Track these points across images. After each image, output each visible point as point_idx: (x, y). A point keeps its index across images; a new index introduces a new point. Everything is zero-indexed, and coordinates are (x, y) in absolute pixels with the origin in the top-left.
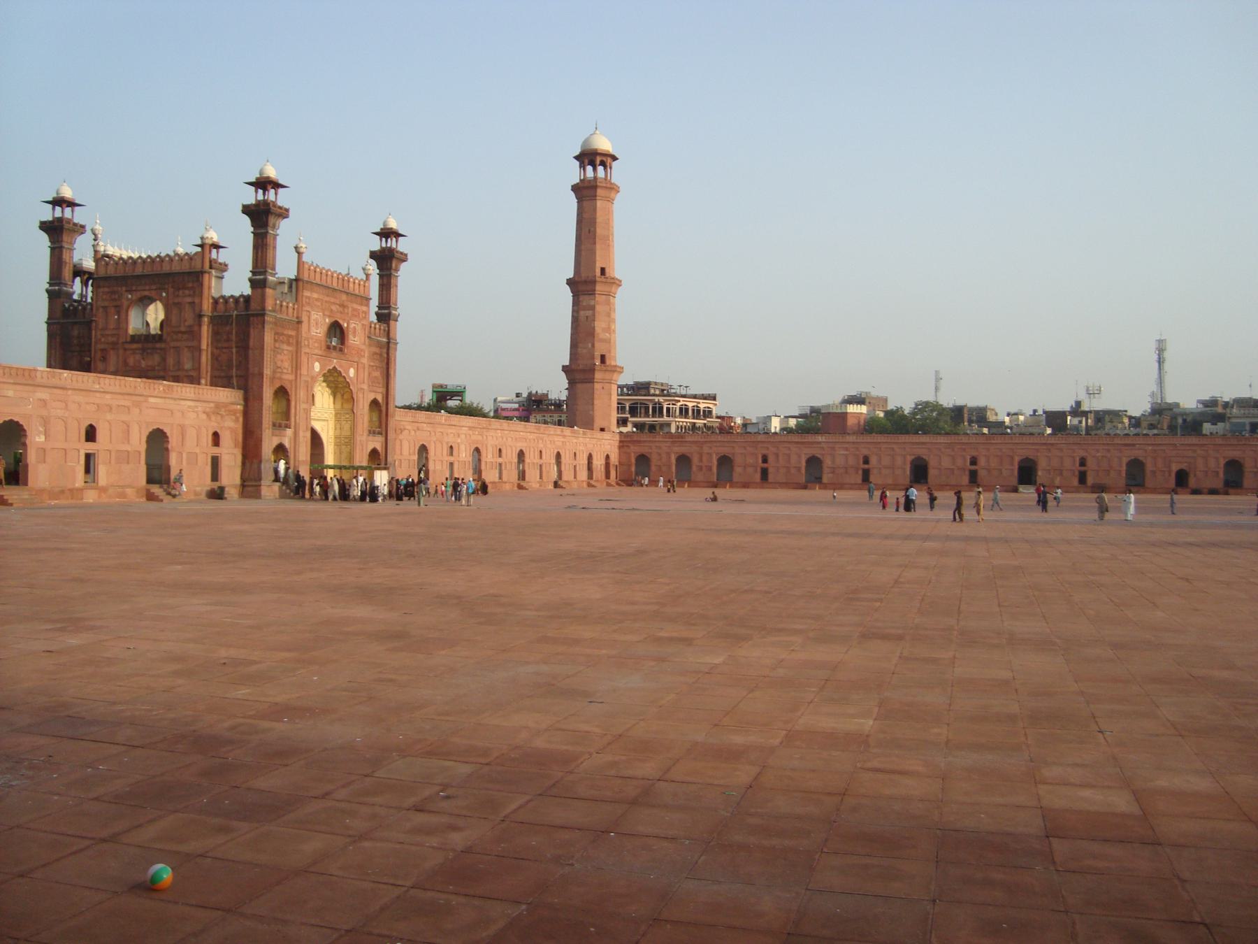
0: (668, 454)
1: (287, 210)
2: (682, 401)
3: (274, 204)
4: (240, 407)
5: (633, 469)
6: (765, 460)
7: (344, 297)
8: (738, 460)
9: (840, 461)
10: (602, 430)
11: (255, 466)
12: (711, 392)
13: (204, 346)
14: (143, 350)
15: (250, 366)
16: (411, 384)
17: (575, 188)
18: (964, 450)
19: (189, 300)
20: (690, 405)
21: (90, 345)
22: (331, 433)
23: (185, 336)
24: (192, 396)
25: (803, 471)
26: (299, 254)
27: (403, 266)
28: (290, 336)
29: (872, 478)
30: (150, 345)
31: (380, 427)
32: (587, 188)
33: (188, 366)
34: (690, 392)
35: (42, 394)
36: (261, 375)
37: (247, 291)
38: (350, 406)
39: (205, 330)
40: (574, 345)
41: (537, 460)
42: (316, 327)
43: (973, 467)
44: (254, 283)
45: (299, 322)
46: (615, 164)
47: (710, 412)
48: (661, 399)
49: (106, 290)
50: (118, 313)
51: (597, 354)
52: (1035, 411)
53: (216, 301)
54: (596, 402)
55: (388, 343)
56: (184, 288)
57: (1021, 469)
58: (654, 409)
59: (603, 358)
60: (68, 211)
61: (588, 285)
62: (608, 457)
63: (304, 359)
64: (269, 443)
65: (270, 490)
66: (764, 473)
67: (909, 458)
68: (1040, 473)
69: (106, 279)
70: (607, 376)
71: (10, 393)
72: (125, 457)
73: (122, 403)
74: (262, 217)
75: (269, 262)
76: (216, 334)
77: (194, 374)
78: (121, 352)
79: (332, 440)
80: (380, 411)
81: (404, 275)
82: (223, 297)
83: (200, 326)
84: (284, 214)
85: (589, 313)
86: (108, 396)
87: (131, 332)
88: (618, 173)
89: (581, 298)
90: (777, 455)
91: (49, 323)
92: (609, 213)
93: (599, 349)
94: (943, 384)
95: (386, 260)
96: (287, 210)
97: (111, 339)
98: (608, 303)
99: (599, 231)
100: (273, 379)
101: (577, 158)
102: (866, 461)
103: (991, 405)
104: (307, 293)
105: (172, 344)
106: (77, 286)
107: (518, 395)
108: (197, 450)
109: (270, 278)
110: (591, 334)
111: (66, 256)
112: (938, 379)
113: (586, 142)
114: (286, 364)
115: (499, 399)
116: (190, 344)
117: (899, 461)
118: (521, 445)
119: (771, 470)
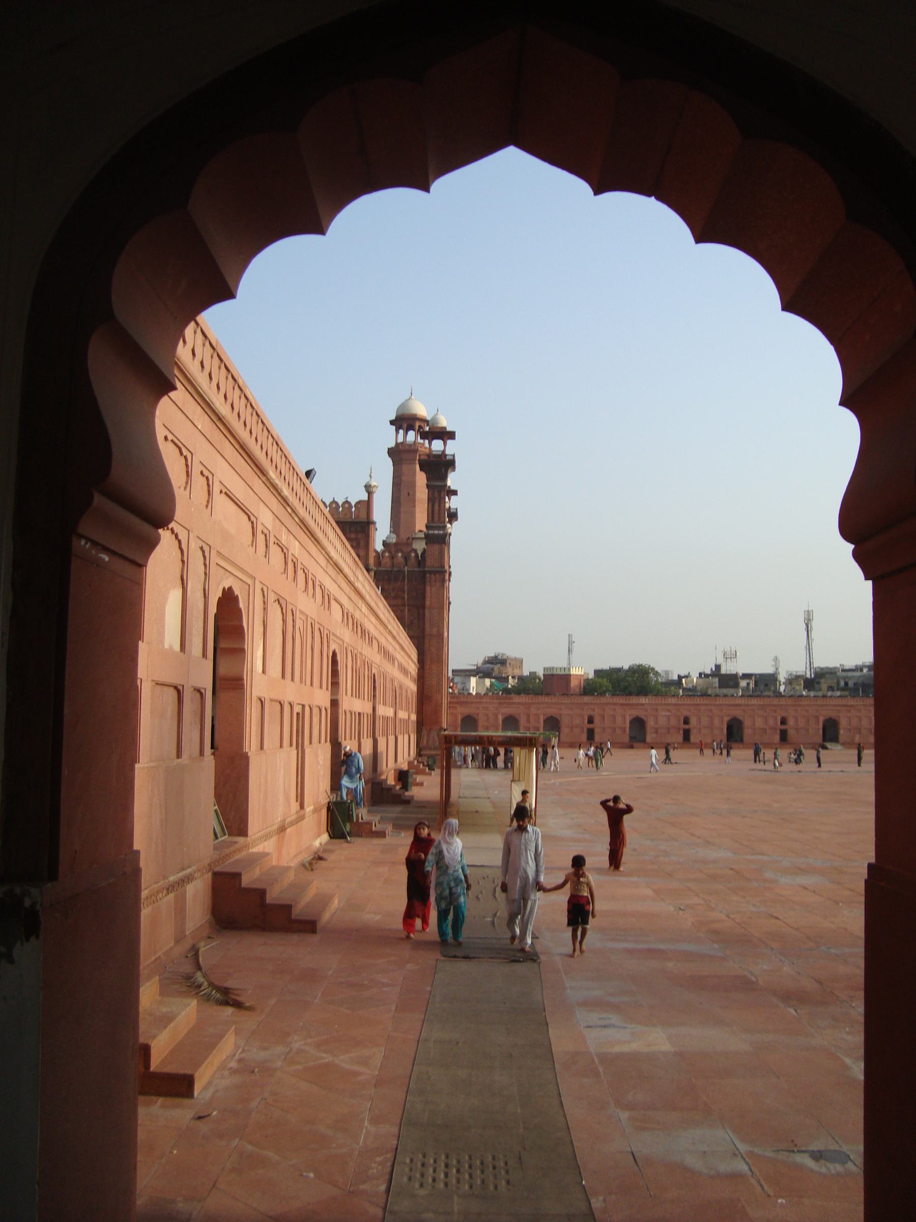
0: (496, 715)
6: (591, 720)
8: (565, 721)
9: (662, 721)
15: (427, 626)
17: (391, 452)
18: (775, 711)
25: (628, 729)
43: (784, 727)
52: (700, 674)
57: (730, 728)
66: (591, 734)
67: (726, 719)
68: (842, 732)
94: (575, 647)
101: (392, 423)
102: (686, 721)
112: (571, 643)
113: (403, 406)
119: (597, 731)
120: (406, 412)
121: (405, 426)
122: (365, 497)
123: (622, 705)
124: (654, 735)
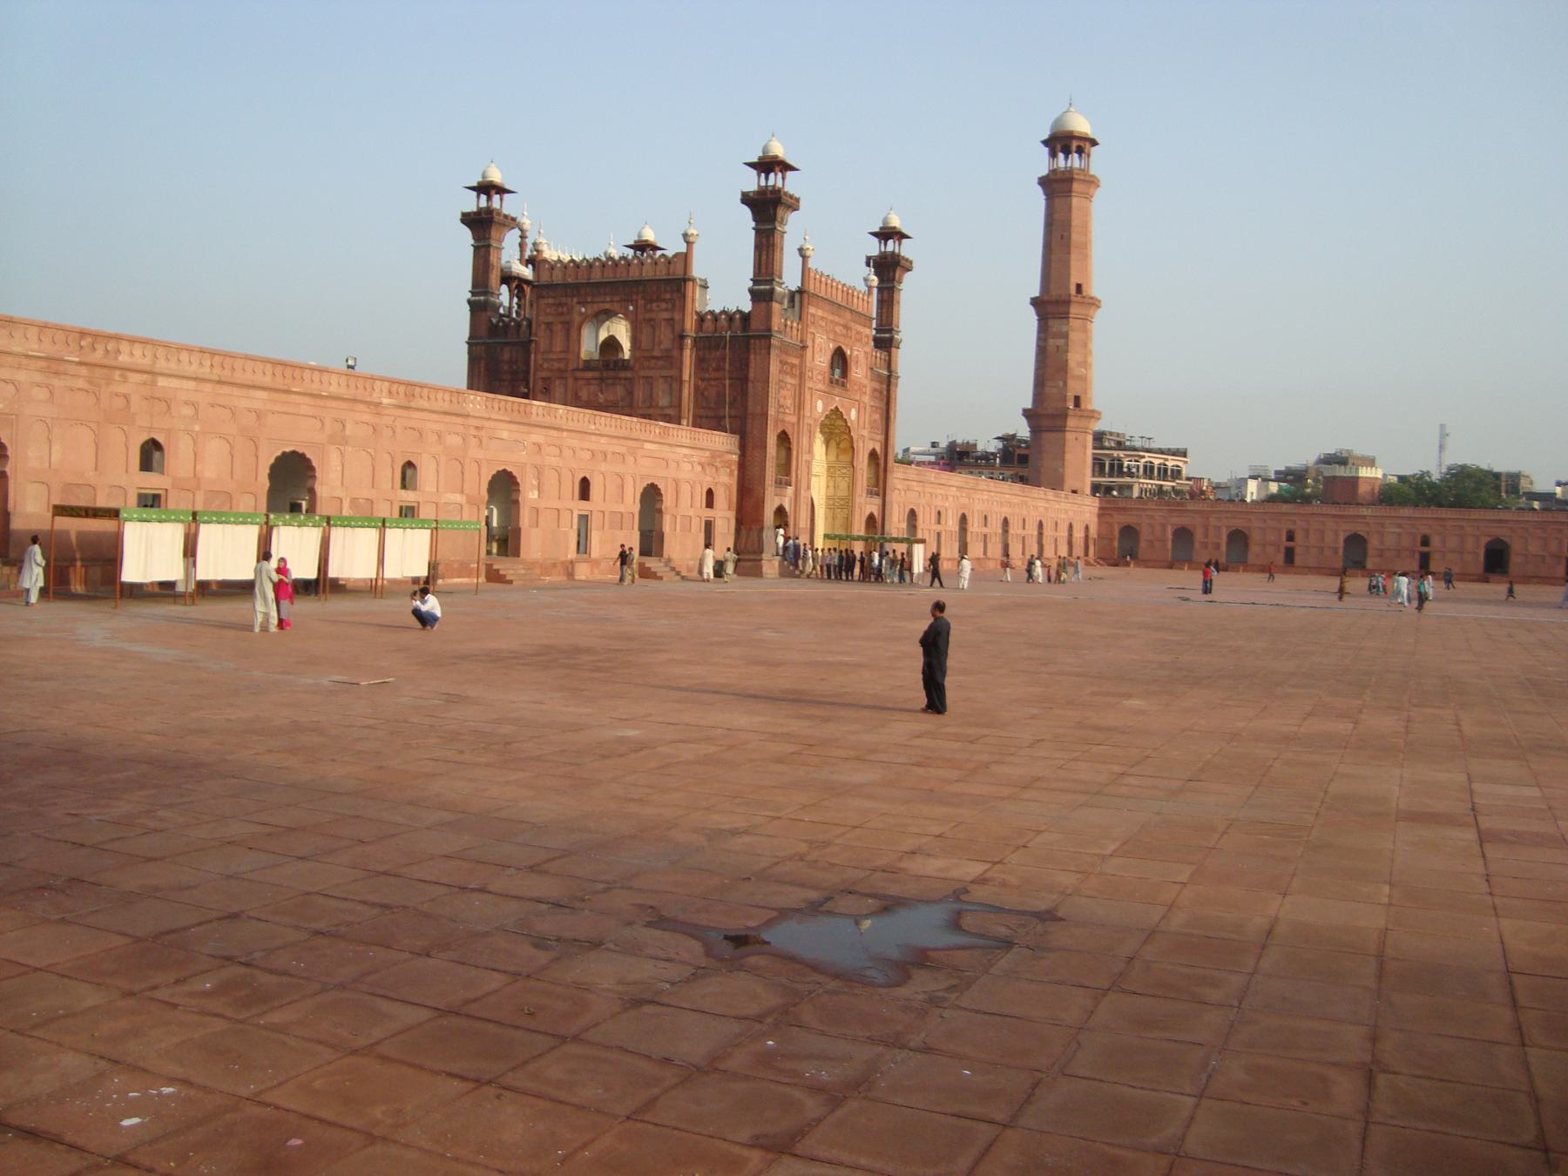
0: (1164, 527)
1: (798, 200)
2: (1148, 457)
4: (735, 458)
5: (1116, 544)
6: (1291, 537)
7: (848, 315)
8: (1255, 536)
10: (1074, 492)
11: (754, 534)
13: (686, 377)
14: (602, 379)
16: (916, 431)
17: (1044, 182)
18: (1560, 531)
19: (666, 315)
20: (1156, 462)
21: (528, 372)
22: (823, 492)
23: (661, 363)
24: (687, 442)
26: (804, 257)
27: (907, 276)
28: (793, 366)
30: (611, 373)
31: (877, 485)
32: (1057, 181)
33: (663, 401)
34: (1154, 445)
35: (537, 437)
36: (765, 415)
37: (746, 306)
38: (846, 458)
39: (688, 356)
40: (1040, 382)
41: (1020, 531)
44: (756, 295)
45: (804, 348)
46: (1094, 150)
47: (1179, 472)
48: (1121, 454)
49: (551, 301)
50: (568, 331)
51: (1070, 395)
53: (701, 318)
54: (1068, 456)
55: (889, 377)
56: (659, 299)
58: (1112, 466)
59: (1077, 400)
60: (496, 198)
61: (1058, 305)
62: (1087, 528)
63: (808, 397)
65: (771, 565)
66: (1290, 555)
67: (1485, 540)
69: (551, 287)
70: (1083, 423)
71: (505, 435)
72: (619, 520)
73: (618, 449)
74: (767, 208)
75: (776, 267)
76: (700, 362)
77: (671, 412)
78: (570, 381)
79: (823, 502)
80: (878, 465)
81: (909, 287)
82: (712, 313)
83: (681, 349)
84: (793, 204)
85: (1061, 342)
86: (603, 440)
87: (583, 356)
88: (1098, 163)
89: (1051, 322)
90: (1307, 531)
91: (471, 344)
92: (1086, 214)
93: (1073, 389)
95: (888, 268)
96: (798, 200)
97: (556, 365)
98: (1085, 330)
99: (1075, 236)
101: (1045, 143)
102: (1425, 541)
103: (1525, 470)
104: (812, 310)
105: (642, 373)
106: (504, 296)
107: (934, 445)
108: (691, 513)
109: (778, 289)
110: (1063, 368)
111: (493, 258)
112: (1444, 435)
113: (1058, 121)
114: (789, 402)
115: (913, 449)
116: (664, 373)
117: (1470, 544)
118: (1006, 511)
119: (1298, 550)
121: (1059, 147)
122: (683, 248)
123: (1334, 516)
124: (1377, 560)
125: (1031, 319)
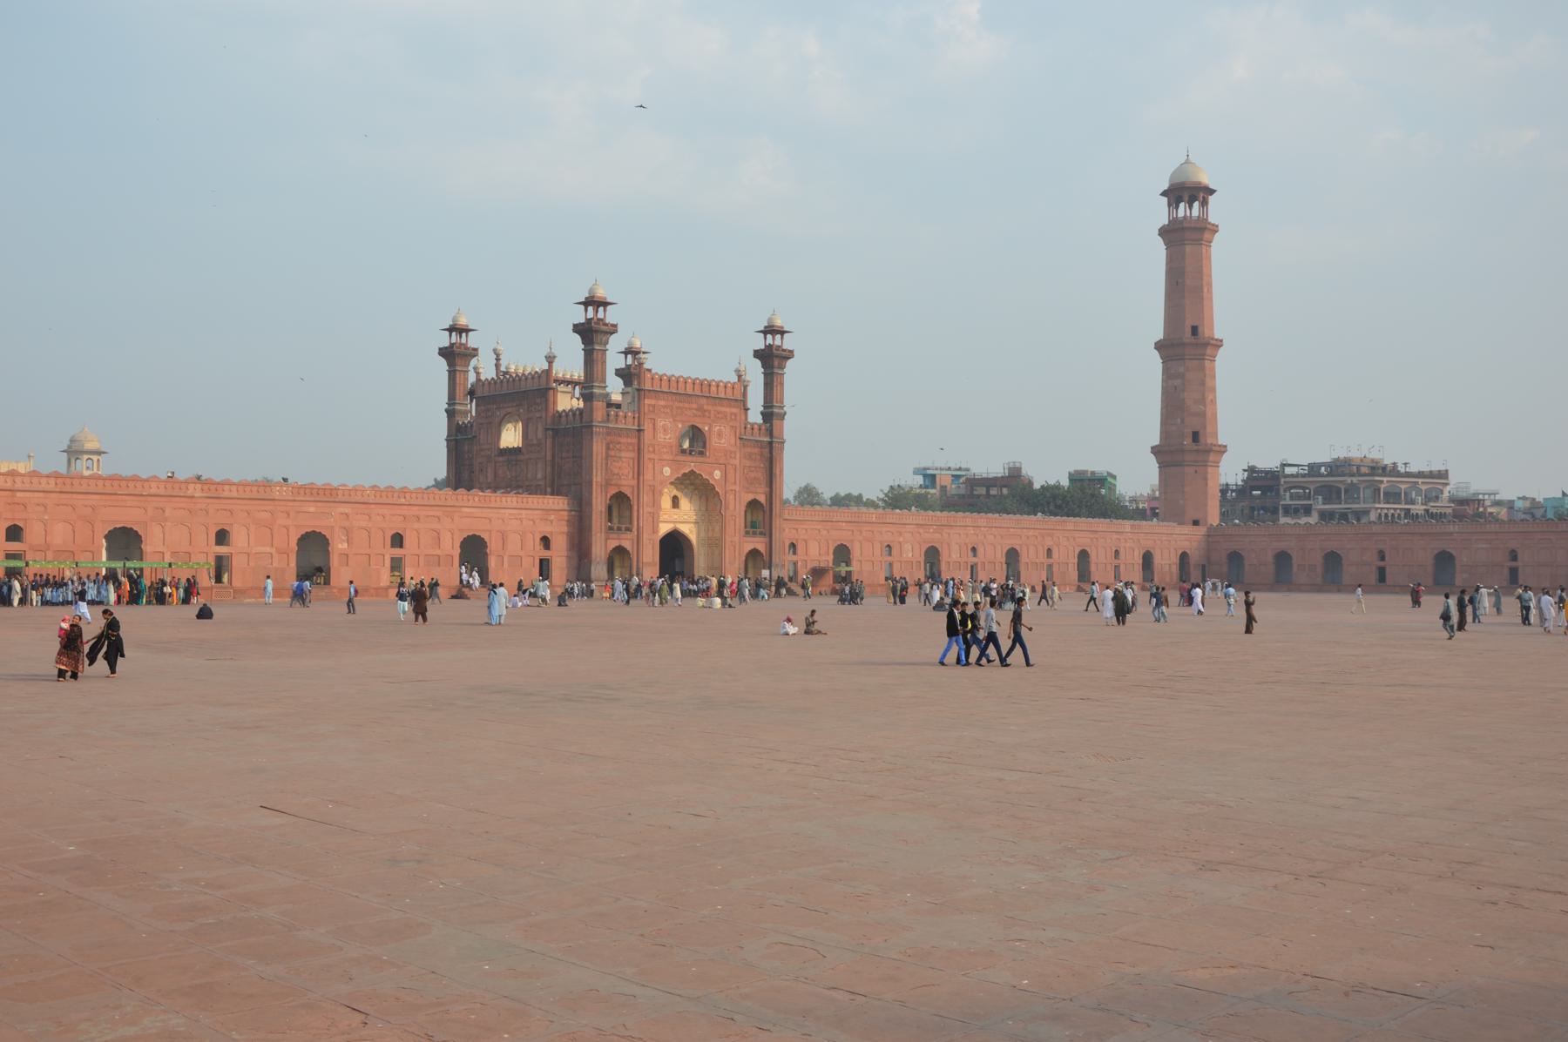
3: (465, 345)
7: (704, 401)
12: (1436, 467)
17: (1163, 232)
24: (515, 505)
29: (1388, 577)
36: (590, 483)
42: (665, 431)
53: (560, 415)
55: (771, 443)
61: (1186, 347)
64: (600, 548)
88: (1217, 211)
96: (615, 326)
100: (608, 484)
101: (1164, 194)
120: (1177, 180)
122: (546, 366)
125: (1154, 364)
